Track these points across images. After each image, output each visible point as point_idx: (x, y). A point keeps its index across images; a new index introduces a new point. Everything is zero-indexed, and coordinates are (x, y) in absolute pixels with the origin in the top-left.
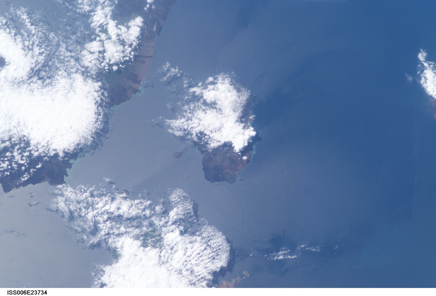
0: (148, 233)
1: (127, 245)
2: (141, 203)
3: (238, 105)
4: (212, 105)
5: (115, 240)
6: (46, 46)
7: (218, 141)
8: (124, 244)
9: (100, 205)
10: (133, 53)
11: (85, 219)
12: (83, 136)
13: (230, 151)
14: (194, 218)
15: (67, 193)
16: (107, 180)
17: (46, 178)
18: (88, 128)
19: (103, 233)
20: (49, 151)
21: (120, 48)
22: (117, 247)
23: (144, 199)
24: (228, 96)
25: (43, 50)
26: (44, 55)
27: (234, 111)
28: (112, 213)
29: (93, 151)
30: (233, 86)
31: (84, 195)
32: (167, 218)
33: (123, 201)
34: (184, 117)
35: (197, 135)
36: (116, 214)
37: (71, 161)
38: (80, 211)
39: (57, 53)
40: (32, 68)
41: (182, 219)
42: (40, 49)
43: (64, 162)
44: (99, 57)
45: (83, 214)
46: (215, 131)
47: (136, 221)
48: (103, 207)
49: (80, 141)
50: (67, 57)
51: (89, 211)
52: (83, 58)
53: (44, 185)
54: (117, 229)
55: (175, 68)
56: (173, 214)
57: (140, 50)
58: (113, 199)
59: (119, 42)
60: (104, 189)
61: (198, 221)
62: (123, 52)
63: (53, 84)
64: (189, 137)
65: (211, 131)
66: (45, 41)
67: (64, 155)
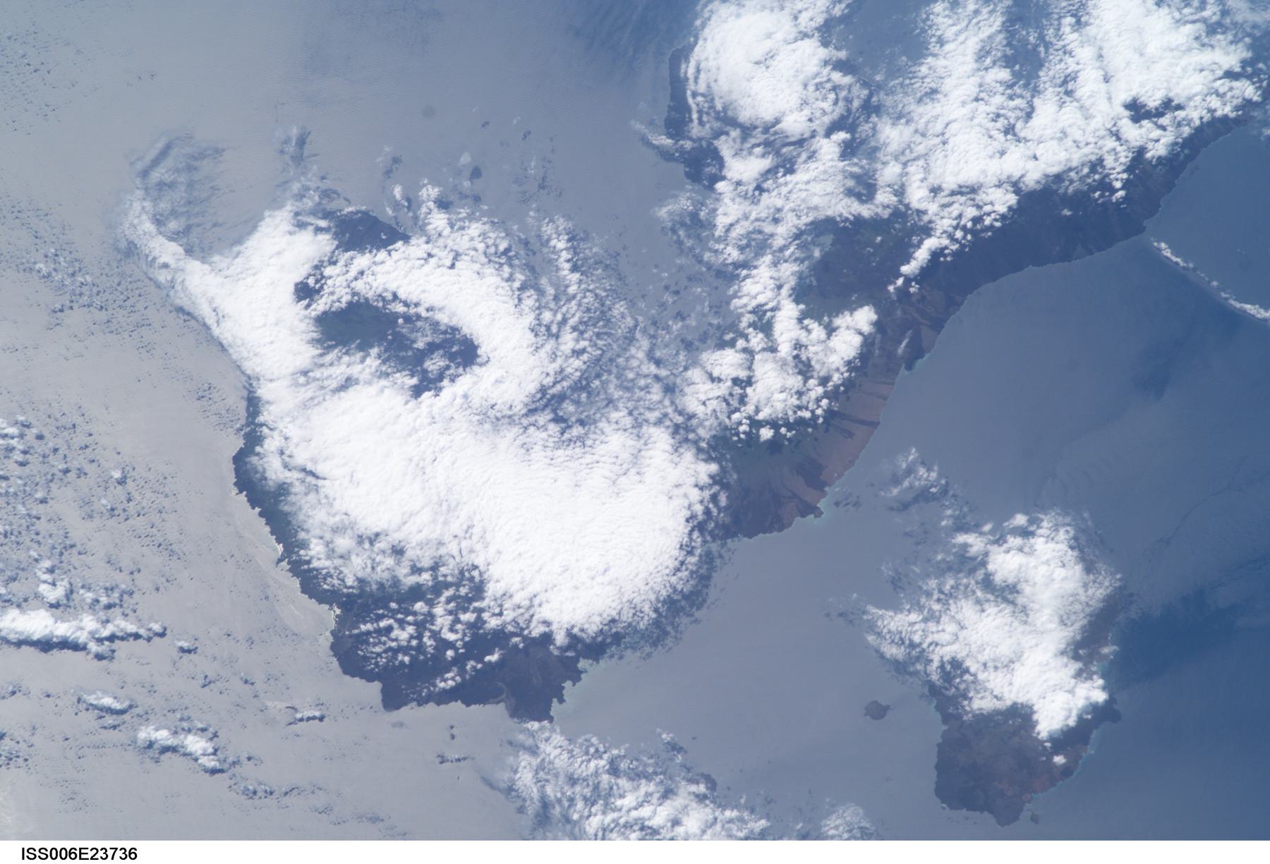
6: (598, 335)
10: (825, 402)
21: (795, 382)
25: (586, 343)
26: (585, 357)
39: (620, 360)
40: (543, 386)
42: (577, 341)
44: (731, 395)
50: (646, 376)
52: (687, 390)
55: (929, 470)
59: (796, 366)
62: (800, 394)
63: (589, 442)
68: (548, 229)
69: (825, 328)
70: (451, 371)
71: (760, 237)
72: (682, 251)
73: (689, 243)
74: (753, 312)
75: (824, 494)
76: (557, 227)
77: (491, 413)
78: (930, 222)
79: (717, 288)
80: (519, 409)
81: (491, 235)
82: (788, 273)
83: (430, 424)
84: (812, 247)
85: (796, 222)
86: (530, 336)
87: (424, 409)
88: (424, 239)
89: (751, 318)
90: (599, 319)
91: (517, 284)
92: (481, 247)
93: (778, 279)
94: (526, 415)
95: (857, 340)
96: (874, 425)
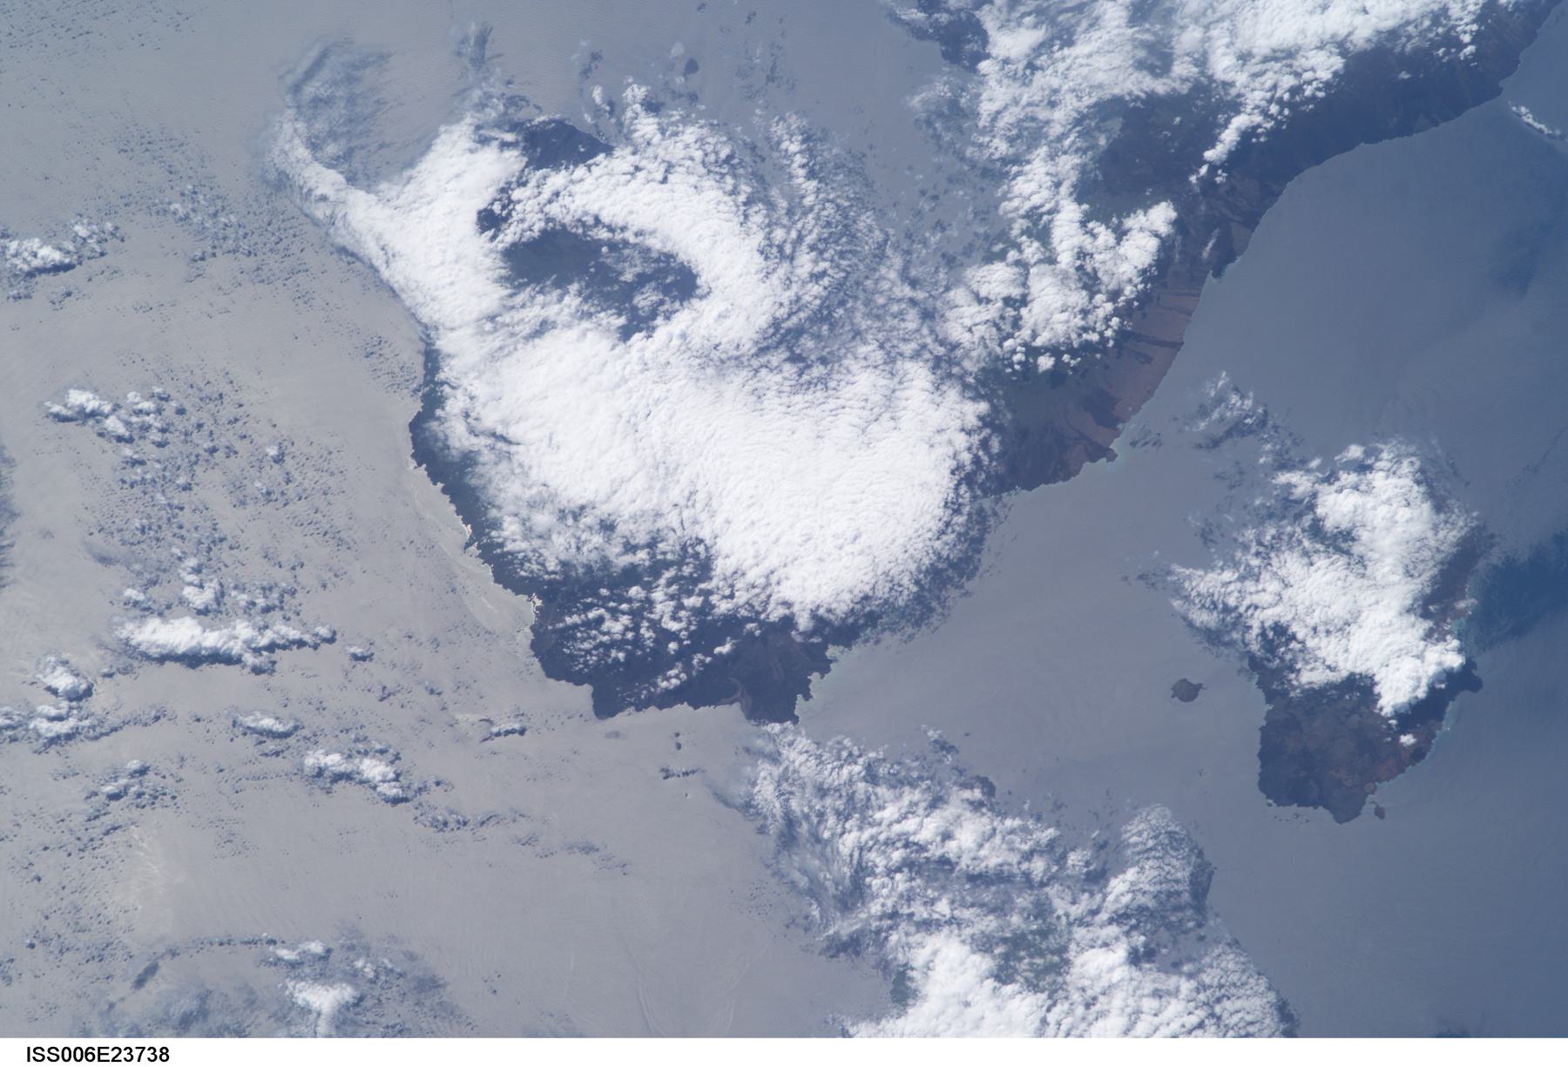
0: (1023, 936)
1: (949, 963)
2: (1025, 830)
3: (1426, 554)
4: (1339, 542)
5: (911, 939)
6: (842, 254)
7: (1329, 667)
8: (937, 961)
9: (890, 813)
10: (1115, 321)
11: (828, 850)
12: (886, 574)
13: (1363, 708)
14: (1189, 912)
15: (793, 755)
16: (930, 733)
17: (739, 694)
18: (911, 551)
19: (875, 908)
20: (767, 602)
21: (1079, 298)
22: (914, 965)
23: (1039, 819)
24: (1398, 517)
25: (826, 265)
26: (826, 281)
27: (1408, 573)
28: (922, 848)
29: (909, 630)
30: (1422, 489)
31: (845, 771)
32: (1099, 897)
33: (968, 814)
34: (1236, 565)
35: (1263, 634)
36: (935, 852)
37: (832, 651)
38: (819, 823)
39: (868, 283)
40: (775, 319)
41: (1147, 909)
42: (816, 262)
43: (808, 648)
44: (1002, 317)
45: (826, 835)
46: (1328, 632)
47: (993, 888)
48: (899, 822)
49: (873, 588)
50: (900, 300)
51: (848, 825)
52: (949, 314)
53: (727, 716)
54: (925, 903)
55: (1243, 397)
56: (1120, 888)
57: (1144, 315)
58: (936, 803)
59: (1080, 279)
60: (916, 764)
61: (1200, 925)
62: (1085, 313)
63: (832, 384)
64: (1236, 636)
65: (1315, 629)
66: (839, 236)
67: (811, 625)
68: (778, 130)
69: (1114, 231)
70: (666, 307)
71: (1033, 125)
72: (940, 147)
73: (947, 137)
74: (1027, 216)
75: (1117, 434)
76: (789, 126)
77: (715, 355)
78: (1239, 95)
79: (983, 190)
80: (748, 347)
81: (710, 140)
82: (1068, 167)
83: (642, 372)
84: (1096, 134)
85: (1077, 104)
86: (759, 259)
87: (634, 354)
88: (630, 149)
89: (1024, 223)
90: (842, 235)
91: (742, 198)
92: (698, 155)
93: (1057, 175)
94: (756, 355)
95: (1153, 243)
96: (1176, 346)
